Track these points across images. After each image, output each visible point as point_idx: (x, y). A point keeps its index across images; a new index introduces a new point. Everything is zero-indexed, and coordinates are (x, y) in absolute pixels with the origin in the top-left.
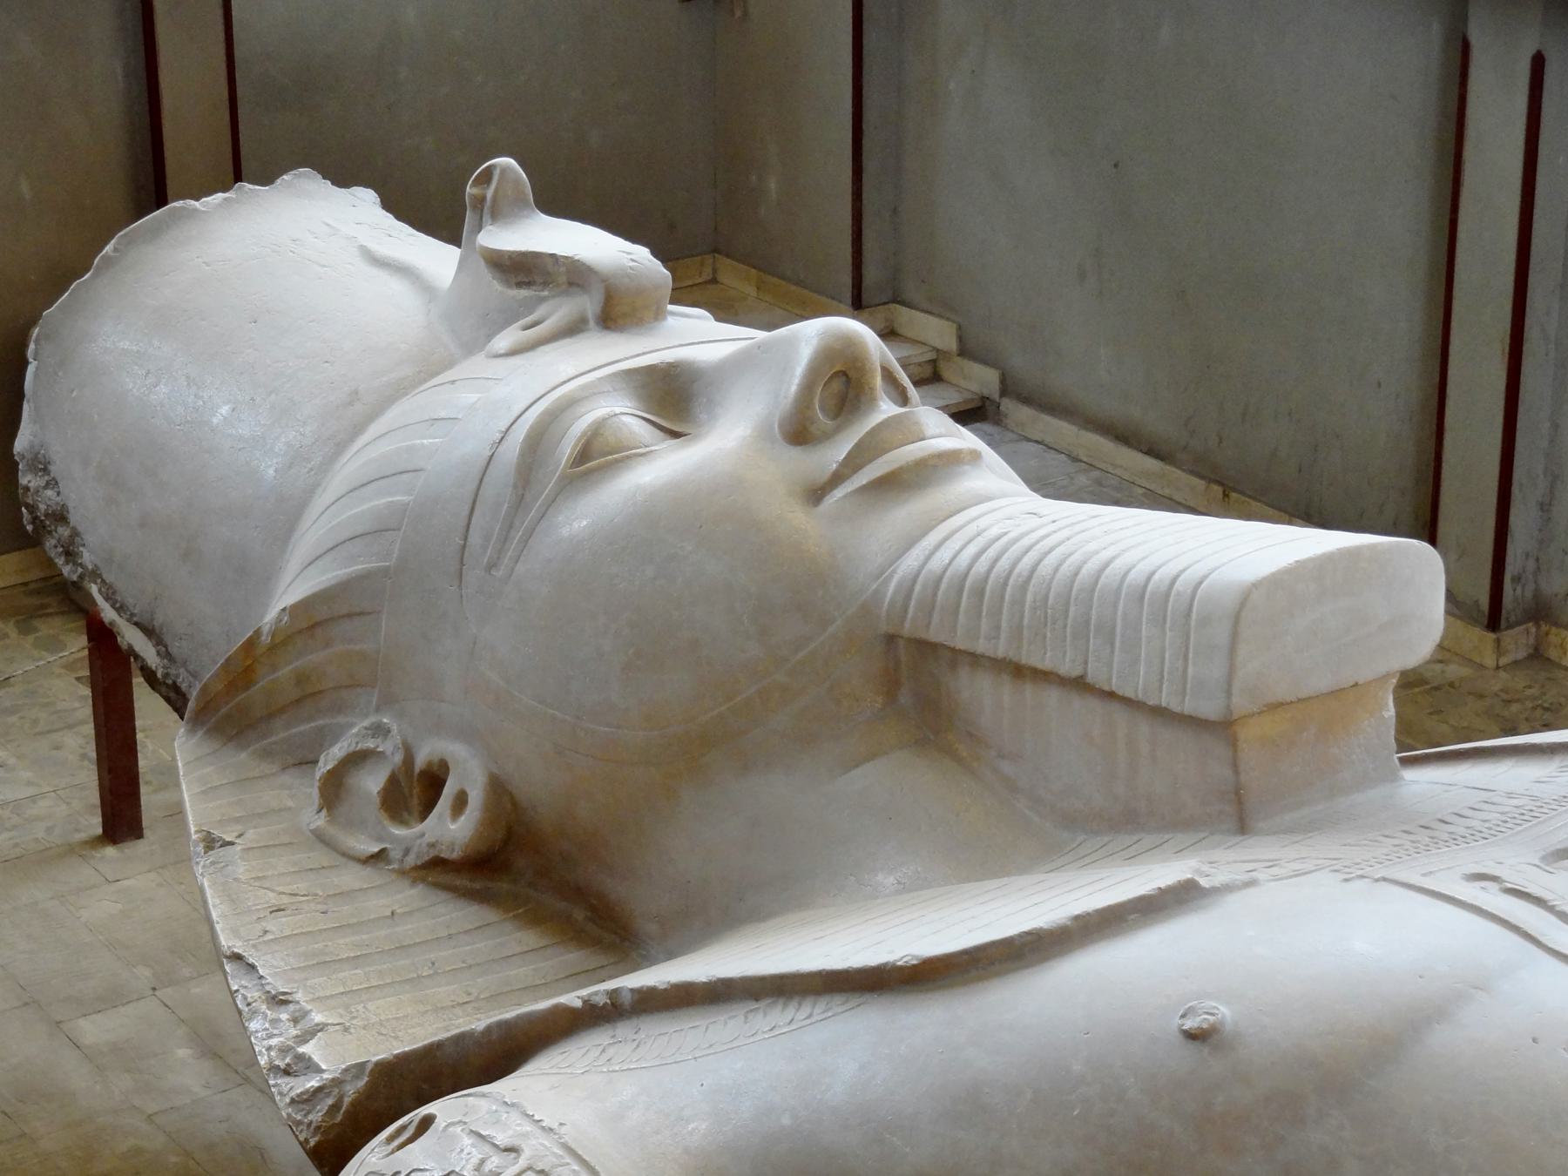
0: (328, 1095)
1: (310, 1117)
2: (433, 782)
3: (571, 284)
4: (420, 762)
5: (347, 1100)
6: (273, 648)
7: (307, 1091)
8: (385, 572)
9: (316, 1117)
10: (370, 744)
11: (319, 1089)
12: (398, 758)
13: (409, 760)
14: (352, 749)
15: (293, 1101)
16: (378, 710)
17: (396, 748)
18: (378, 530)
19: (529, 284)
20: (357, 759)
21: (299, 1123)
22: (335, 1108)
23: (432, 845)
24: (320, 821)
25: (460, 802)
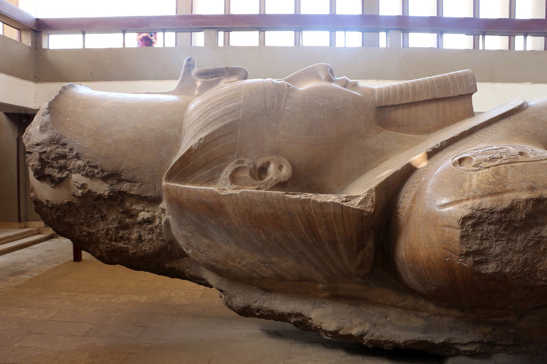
0: (368, 198)
1: (367, 205)
2: (262, 171)
3: (230, 74)
4: (259, 164)
5: (374, 198)
6: (197, 151)
7: (362, 200)
8: (238, 120)
9: (370, 203)
10: (238, 166)
11: (365, 198)
12: (251, 166)
13: (255, 166)
14: (235, 167)
15: (359, 204)
16: (237, 158)
17: (249, 164)
18: (229, 112)
19: (216, 77)
20: (236, 170)
21: (365, 208)
22: (372, 201)
23: (278, 179)
24: (235, 186)
25: (280, 167)
